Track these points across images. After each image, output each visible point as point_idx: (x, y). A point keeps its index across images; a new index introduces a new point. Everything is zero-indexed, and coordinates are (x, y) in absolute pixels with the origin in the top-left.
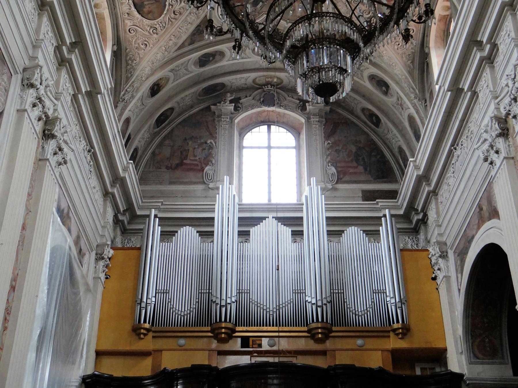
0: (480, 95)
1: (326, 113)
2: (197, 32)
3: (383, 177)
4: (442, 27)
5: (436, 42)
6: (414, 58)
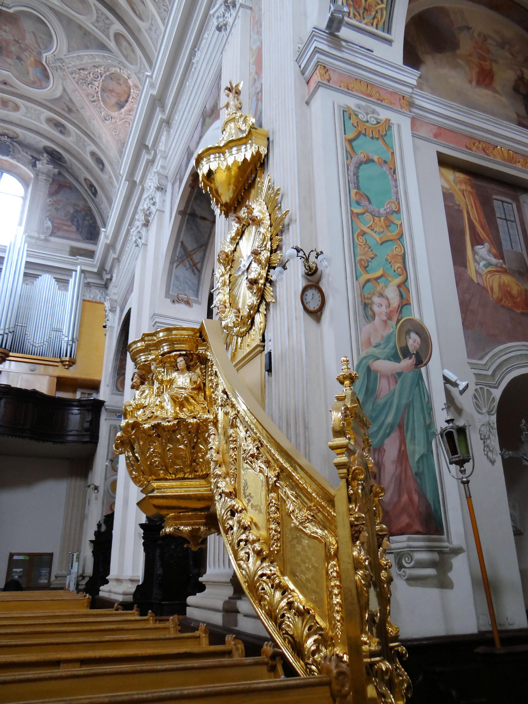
1: (54, 175)
3: (91, 239)
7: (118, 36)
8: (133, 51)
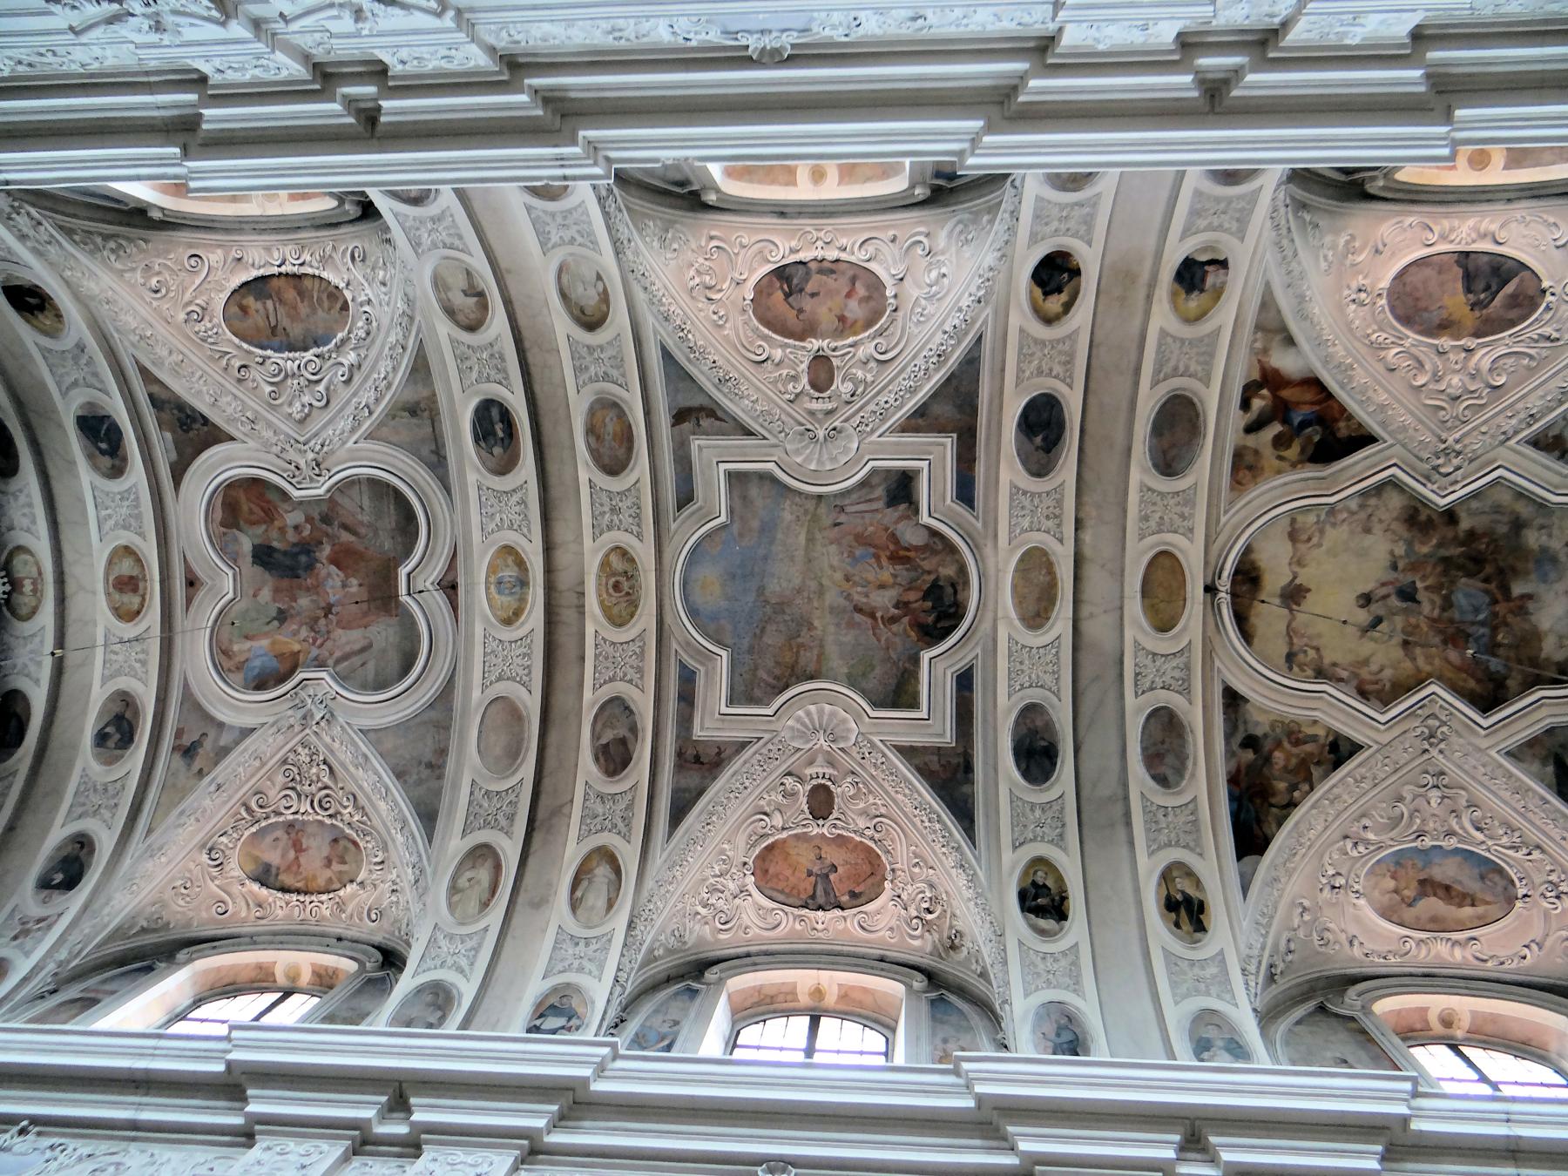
0: (255, 1152)
2: (188, 416)
4: (244, 977)
5: (206, 972)
6: (155, 930)
7: (483, 854)
8: (485, 905)
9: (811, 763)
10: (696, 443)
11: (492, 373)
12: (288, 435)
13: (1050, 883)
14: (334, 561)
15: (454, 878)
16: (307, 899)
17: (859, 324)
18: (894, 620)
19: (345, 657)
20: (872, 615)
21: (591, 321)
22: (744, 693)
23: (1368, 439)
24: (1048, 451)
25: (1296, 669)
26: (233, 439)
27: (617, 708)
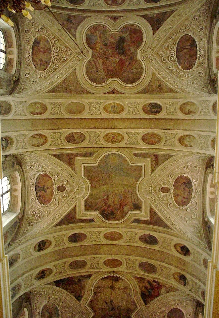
7: (45, 108)
9: (71, 186)
10: (149, 159)
11: (169, 111)
12: (154, 50)
13: (46, 246)
14: (121, 60)
15: (38, 103)
16: (31, 55)
17: (176, 199)
18: (106, 204)
19: (95, 63)
20: (107, 199)
21: (181, 140)
22: (88, 170)
23: (146, 304)
24: (145, 241)
25: (96, 288)
26: (154, 34)
27: (83, 138)
